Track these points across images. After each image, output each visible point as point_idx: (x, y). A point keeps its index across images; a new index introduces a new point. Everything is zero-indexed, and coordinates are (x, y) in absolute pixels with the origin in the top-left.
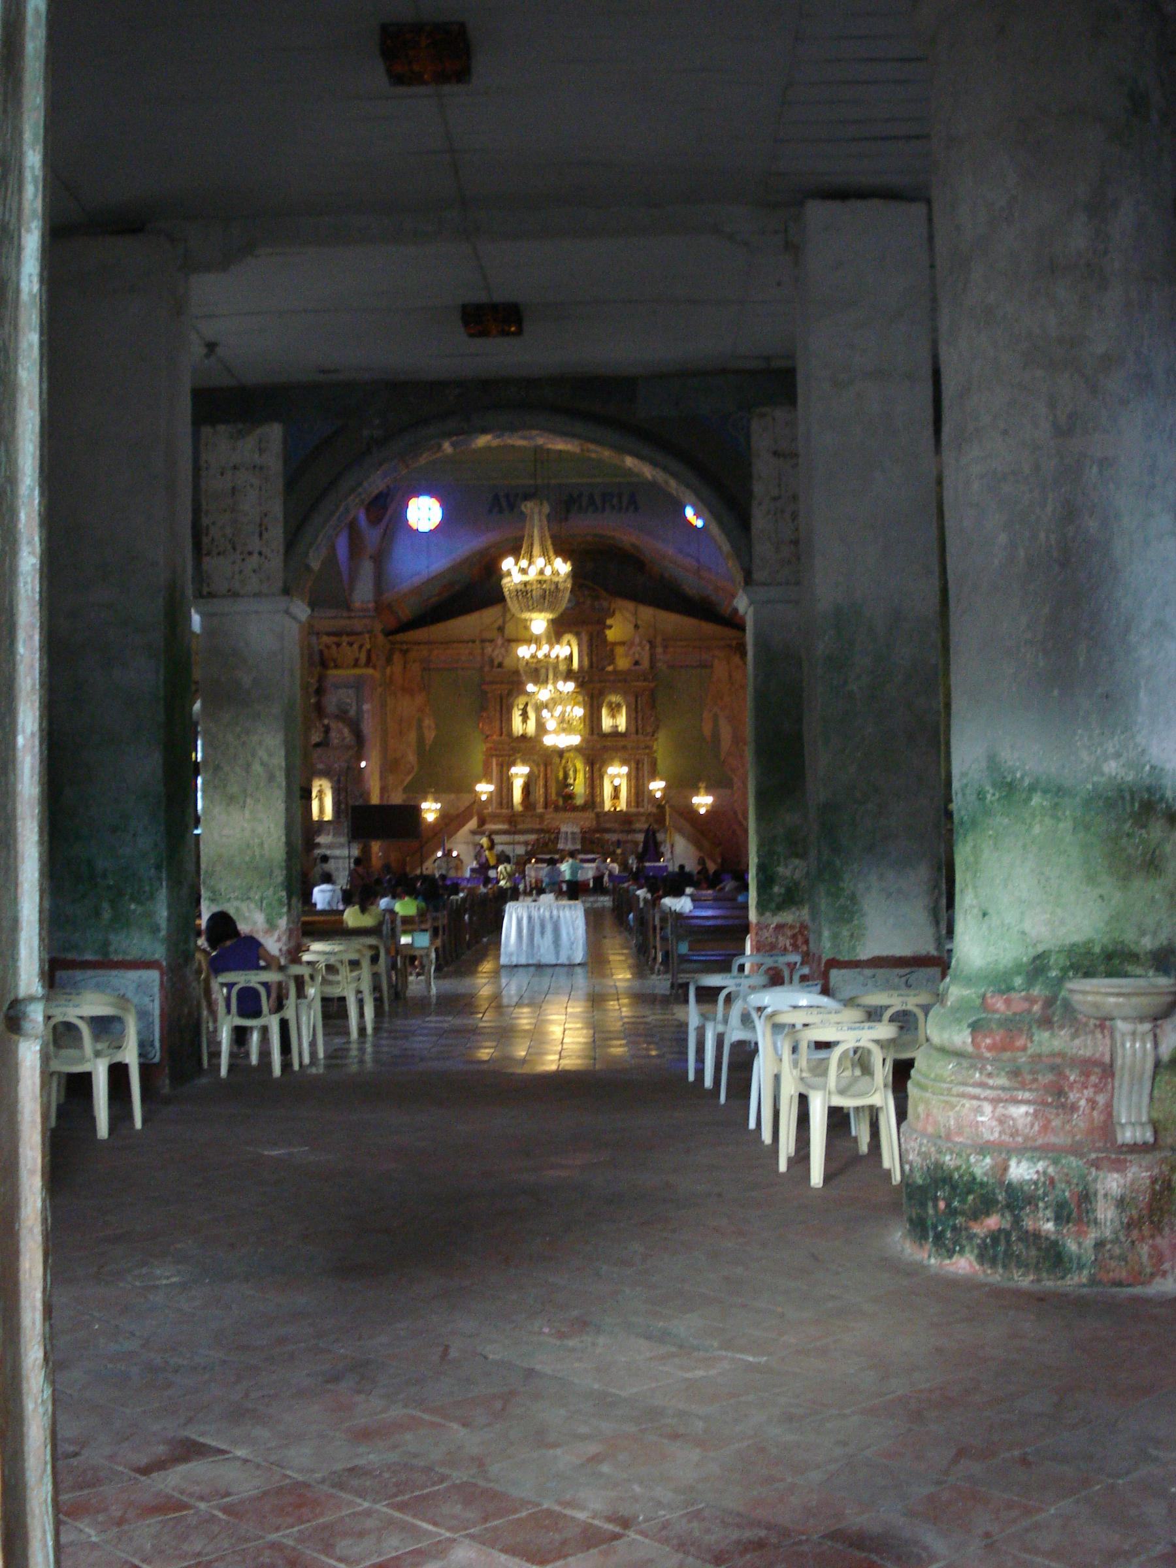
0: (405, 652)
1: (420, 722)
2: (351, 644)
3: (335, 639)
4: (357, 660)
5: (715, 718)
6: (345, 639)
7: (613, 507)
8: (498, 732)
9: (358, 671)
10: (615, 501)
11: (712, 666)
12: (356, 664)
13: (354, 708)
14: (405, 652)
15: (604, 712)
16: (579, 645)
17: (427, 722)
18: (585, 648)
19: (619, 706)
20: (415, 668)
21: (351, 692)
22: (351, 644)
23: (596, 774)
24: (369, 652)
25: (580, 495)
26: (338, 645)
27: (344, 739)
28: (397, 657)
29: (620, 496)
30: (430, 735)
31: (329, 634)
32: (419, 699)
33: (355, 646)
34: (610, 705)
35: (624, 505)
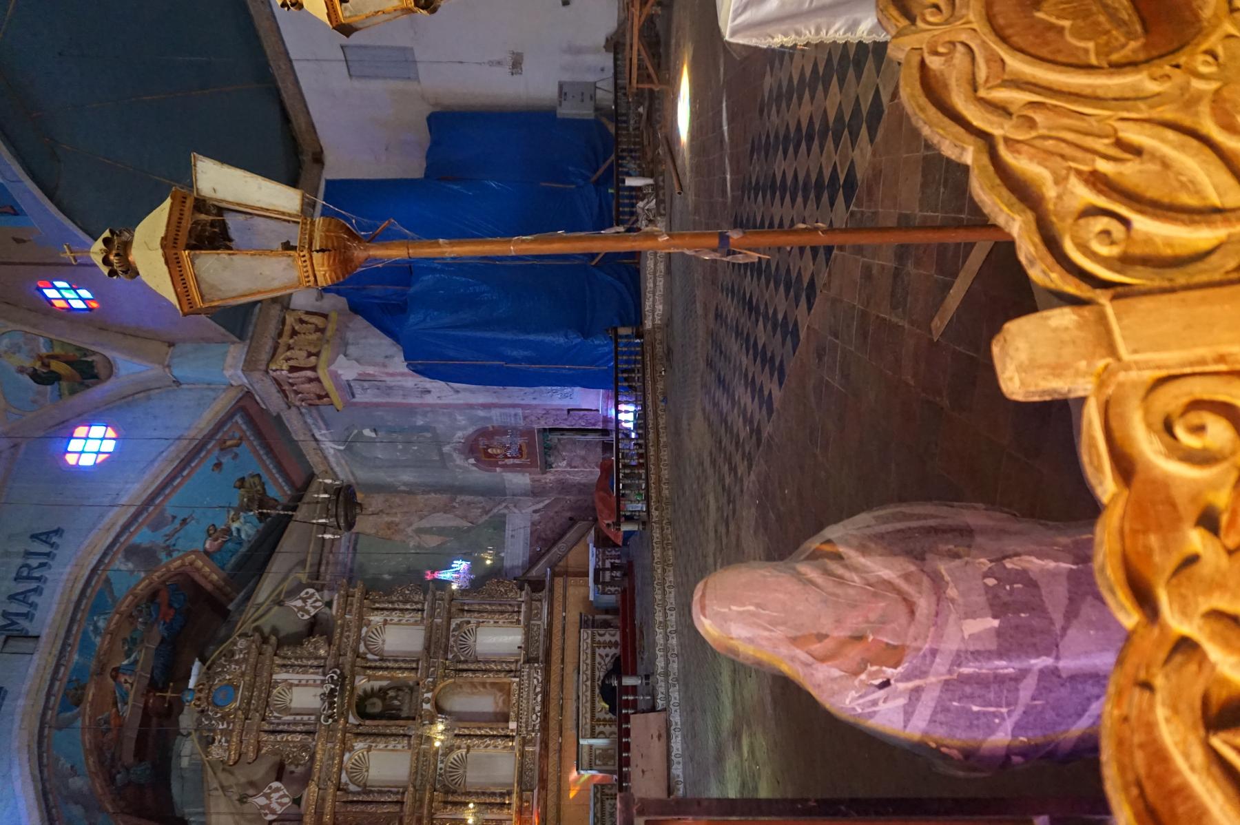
5: (419, 531)
7: (42, 565)
10: (34, 562)
11: (358, 533)
25: (6, 614)
29: (28, 554)
35: (45, 549)
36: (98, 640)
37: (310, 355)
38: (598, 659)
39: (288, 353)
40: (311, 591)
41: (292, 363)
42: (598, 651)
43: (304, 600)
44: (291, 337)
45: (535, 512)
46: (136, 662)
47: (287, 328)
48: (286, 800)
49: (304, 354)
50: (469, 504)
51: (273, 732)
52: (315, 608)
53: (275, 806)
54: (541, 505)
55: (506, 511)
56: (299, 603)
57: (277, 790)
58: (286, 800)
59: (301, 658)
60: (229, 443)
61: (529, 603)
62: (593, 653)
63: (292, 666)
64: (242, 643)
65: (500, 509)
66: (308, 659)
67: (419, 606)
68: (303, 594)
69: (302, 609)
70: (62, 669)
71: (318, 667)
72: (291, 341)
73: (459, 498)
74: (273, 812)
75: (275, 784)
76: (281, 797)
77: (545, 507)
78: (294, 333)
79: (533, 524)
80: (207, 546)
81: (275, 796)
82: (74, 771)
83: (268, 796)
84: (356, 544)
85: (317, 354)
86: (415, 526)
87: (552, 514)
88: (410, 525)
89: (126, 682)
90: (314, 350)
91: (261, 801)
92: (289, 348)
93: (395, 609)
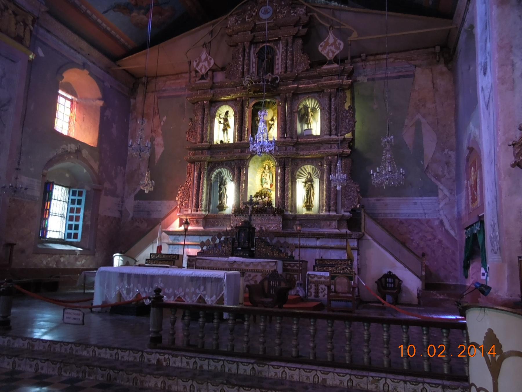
5: (418, 125)
11: (413, 76)
14: (146, 85)
19: (314, 110)
23: (288, 177)
28: (140, 89)
30: (159, 150)
38: (253, 274)
40: (342, 47)
42: (259, 274)
43: (334, 44)
45: (441, 222)
50: (447, 163)
51: (244, 50)
53: (201, 64)
54: (447, 226)
55: (440, 196)
57: (209, 64)
59: (292, 55)
61: (340, 220)
62: (257, 271)
63: (287, 51)
65: (443, 190)
66: (292, 60)
67: (333, 132)
69: (327, 44)
71: (286, 68)
73: (452, 154)
74: (198, 65)
77: (447, 231)
79: (428, 221)
81: (206, 64)
83: (206, 59)
84: (404, 76)
86: (423, 120)
87: (439, 237)
88: (424, 116)
91: (203, 56)
93: (330, 113)
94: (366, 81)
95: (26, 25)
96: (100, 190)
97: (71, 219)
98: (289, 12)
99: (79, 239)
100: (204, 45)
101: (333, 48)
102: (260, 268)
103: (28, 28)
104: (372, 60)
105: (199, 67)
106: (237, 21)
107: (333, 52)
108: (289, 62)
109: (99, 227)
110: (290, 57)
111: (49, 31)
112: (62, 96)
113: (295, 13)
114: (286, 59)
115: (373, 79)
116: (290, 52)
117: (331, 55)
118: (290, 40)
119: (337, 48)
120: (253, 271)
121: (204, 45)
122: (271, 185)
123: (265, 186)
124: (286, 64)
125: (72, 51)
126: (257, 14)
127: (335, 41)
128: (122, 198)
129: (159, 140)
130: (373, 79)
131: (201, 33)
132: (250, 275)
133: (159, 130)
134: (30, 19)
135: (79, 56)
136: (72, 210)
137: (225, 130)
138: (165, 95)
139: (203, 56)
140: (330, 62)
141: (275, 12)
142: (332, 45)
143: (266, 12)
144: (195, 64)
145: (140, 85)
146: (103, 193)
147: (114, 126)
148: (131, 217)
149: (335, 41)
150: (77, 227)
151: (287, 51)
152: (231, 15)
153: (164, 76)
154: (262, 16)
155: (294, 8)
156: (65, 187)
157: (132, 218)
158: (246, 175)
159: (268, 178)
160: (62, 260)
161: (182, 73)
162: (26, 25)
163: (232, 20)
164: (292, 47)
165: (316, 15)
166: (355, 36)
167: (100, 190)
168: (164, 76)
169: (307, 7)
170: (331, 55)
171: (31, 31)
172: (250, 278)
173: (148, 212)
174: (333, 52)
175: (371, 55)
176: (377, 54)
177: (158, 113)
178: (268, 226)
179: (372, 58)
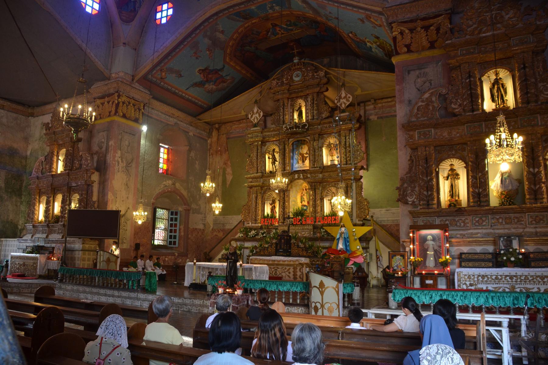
0: (218, 129)
1: (224, 170)
2: (108, 102)
3: (102, 101)
4: (110, 112)
6: (107, 99)
8: (256, 171)
9: (108, 119)
12: (109, 116)
13: (105, 145)
14: (218, 129)
15: (325, 151)
16: (306, 106)
17: (229, 170)
18: (309, 107)
20: (224, 138)
21: (105, 134)
22: (108, 102)
23: (318, 197)
24: (117, 105)
26: (103, 104)
27: (88, 165)
28: (215, 133)
30: (229, 178)
31: (100, 98)
32: (225, 156)
33: (111, 103)
34: (329, 146)
36: (271, 11)
37: (408, 46)
38: (288, 268)
39: (407, 31)
40: (351, 99)
41: (399, 37)
44: (422, 28)
46: (292, 30)
47: (432, 21)
48: (256, 121)
49: (408, 42)
52: (341, 105)
53: (254, 116)
56: (343, 95)
57: (259, 115)
58: (256, 121)
60: (371, 20)
62: (290, 265)
63: (313, 103)
64: (322, 74)
66: (318, 110)
67: (349, 162)
68: (349, 95)
69: (340, 98)
70: (243, 6)
72: (419, 29)
74: (252, 117)
75: (262, 114)
76: (257, 118)
78: (426, 28)
80: (350, 35)
81: (257, 115)
82: (222, 32)
83: (257, 112)
85: (409, 51)
89: (279, 30)
90: (412, 48)
91: (255, 110)
92: (411, 30)
93: (346, 148)
94: (376, 119)
95: (140, 110)
96: (189, 210)
97: (171, 231)
98: (313, 75)
99: (177, 245)
100: (256, 102)
101: (345, 101)
102: (292, 263)
103: (141, 112)
104: (380, 103)
105: (253, 118)
106: (277, 83)
107: (345, 104)
108: (315, 112)
109: (190, 236)
110: (315, 108)
111: (153, 109)
112: (162, 147)
113: (318, 75)
114: (313, 110)
115: (381, 118)
116: (316, 104)
117: (343, 106)
118: (315, 95)
119: (348, 100)
120: (288, 265)
121: (256, 102)
122: (308, 203)
123: (303, 203)
124: (313, 112)
125: (167, 117)
126: (292, 78)
127: (346, 95)
128: (205, 214)
129: (229, 170)
130: (381, 118)
131: (253, 93)
132: (286, 268)
133: (229, 163)
134: (142, 105)
135: (171, 119)
136: (171, 225)
137: (273, 163)
138: (231, 136)
139: (255, 110)
140: (343, 111)
141: (303, 75)
142: (344, 98)
143: (297, 76)
144: (250, 116)
145: (214, 130)
146: (191, 212)
147: (197, 163)
148: (211, 228)
149: (346, 95)
150: (175, 237)
151: (313, 103)
152: (274, 79)
153: (230, 122)
154: (296, 79)
155: (316, 72)
156: (167, 209)
157: (212, 230)
158: (288, 196)
159: (305, 197)
160: (167, 259)
161: (243, 119)
162: (140, 110)
163: (274, 82)
164: (317, 100)
165: (331, 76)
166: (359, 92)
167: (189, 210)
168: (230, 122)
169: (326, 71)
170: (343, 106)
171: (143, 113)
172: (286, 270)
173: (223, 224)
174: (345, 104)
175: (379, 99)
176: (382, 99)
177: (228, 150)
178: (303, 233)
179: (380, 101)
